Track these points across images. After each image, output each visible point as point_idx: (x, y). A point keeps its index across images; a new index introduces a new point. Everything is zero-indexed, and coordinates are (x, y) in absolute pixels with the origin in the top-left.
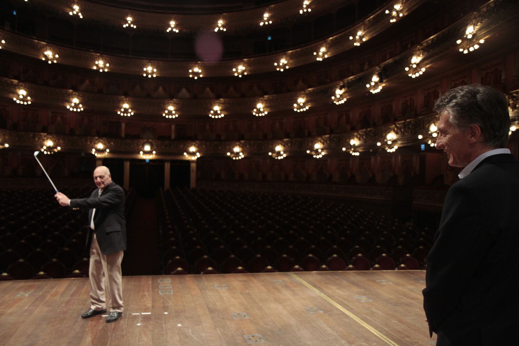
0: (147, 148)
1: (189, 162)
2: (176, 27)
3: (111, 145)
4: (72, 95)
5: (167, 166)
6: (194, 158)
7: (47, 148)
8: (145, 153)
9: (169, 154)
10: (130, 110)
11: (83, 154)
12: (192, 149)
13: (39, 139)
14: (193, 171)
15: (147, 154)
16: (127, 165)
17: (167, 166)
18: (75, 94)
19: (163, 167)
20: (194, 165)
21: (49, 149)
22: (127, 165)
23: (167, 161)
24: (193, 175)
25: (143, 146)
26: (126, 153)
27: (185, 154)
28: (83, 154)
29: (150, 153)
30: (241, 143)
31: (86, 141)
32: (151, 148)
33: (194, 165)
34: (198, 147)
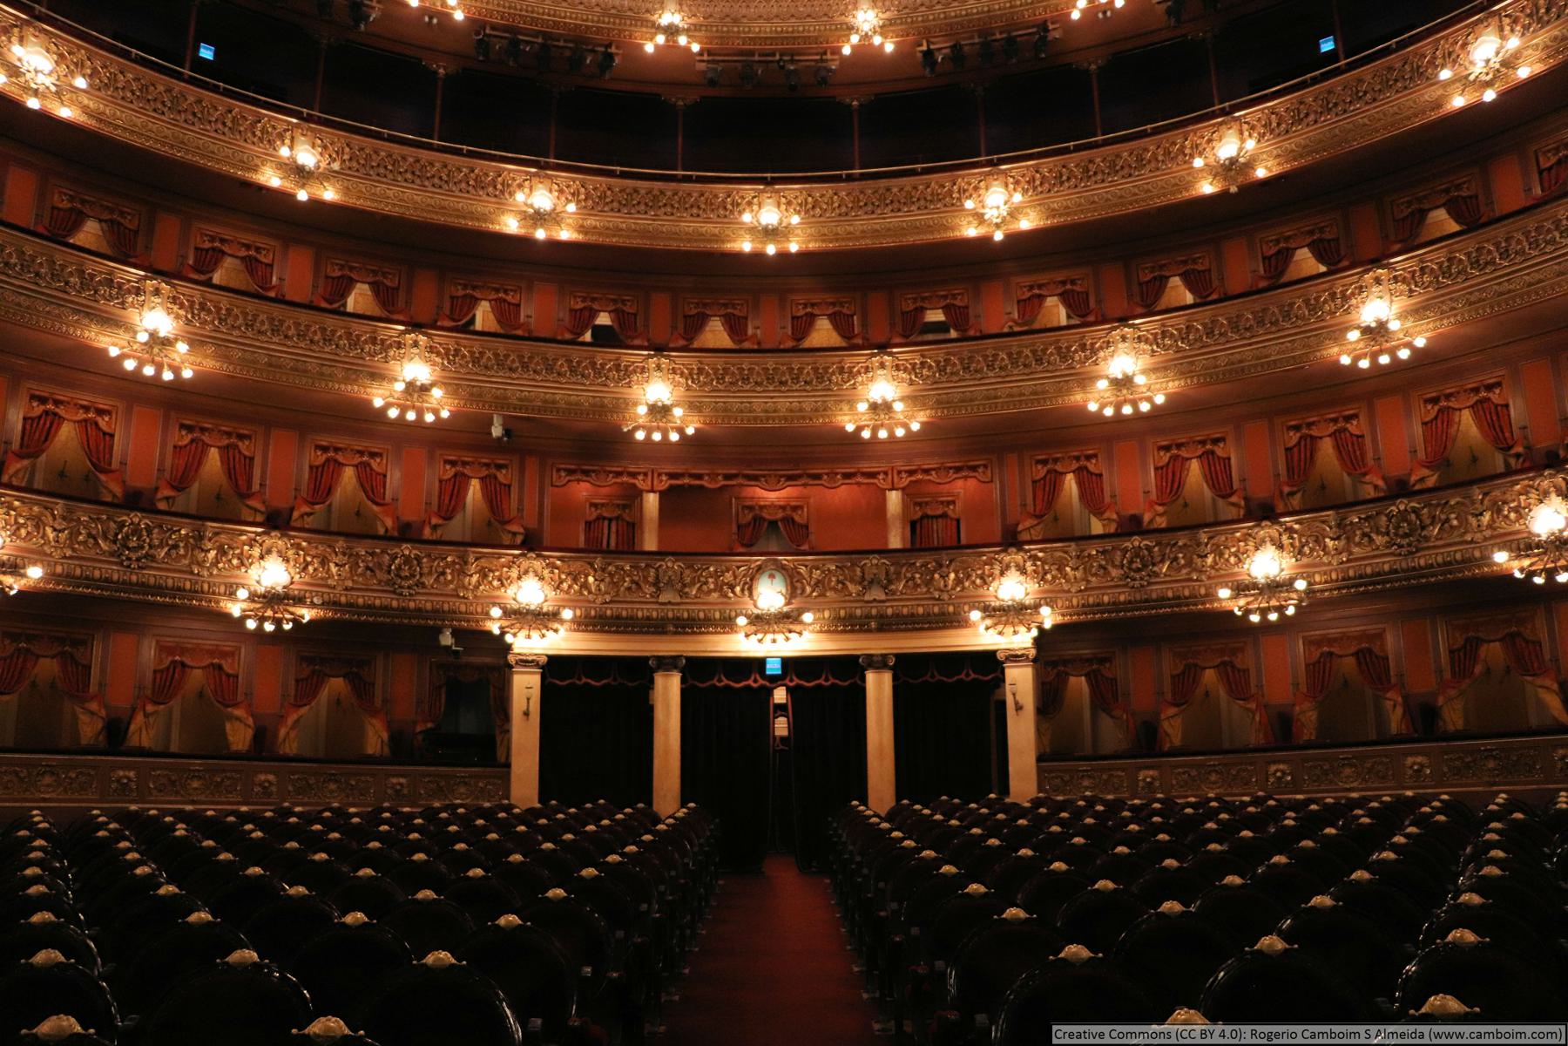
0: (770, 595)
1: (989, 663)
2: (884, 30)
3: (585, 585)
4: (399, 345)
5: (878, 688)
6: (1022, 639)
7: (253, 597)
8: (761, 622)
9: (886, 625)
10: (678, 412)
11: (447, 639)
12: (1012, 587)
13: (222, 552)
14: (1019, 708)
15: (772, 625)
16: (668, 691)
17: (878, 688)
18: (416, 344)
19: (858, 695)
20: (1020, 681)
21: (272, 599)
22: (668, 691)
23: (878, 663)
24: (1022, 733)
25: (750, 589)
26: (656, 627)
27: (975, 615)
28: (447, 639)
29: (787, 620)
30: (1290, 530)
31: (462, 572)
32: (790, 599)
33: (1020, 681)
34: (1041, 576)
